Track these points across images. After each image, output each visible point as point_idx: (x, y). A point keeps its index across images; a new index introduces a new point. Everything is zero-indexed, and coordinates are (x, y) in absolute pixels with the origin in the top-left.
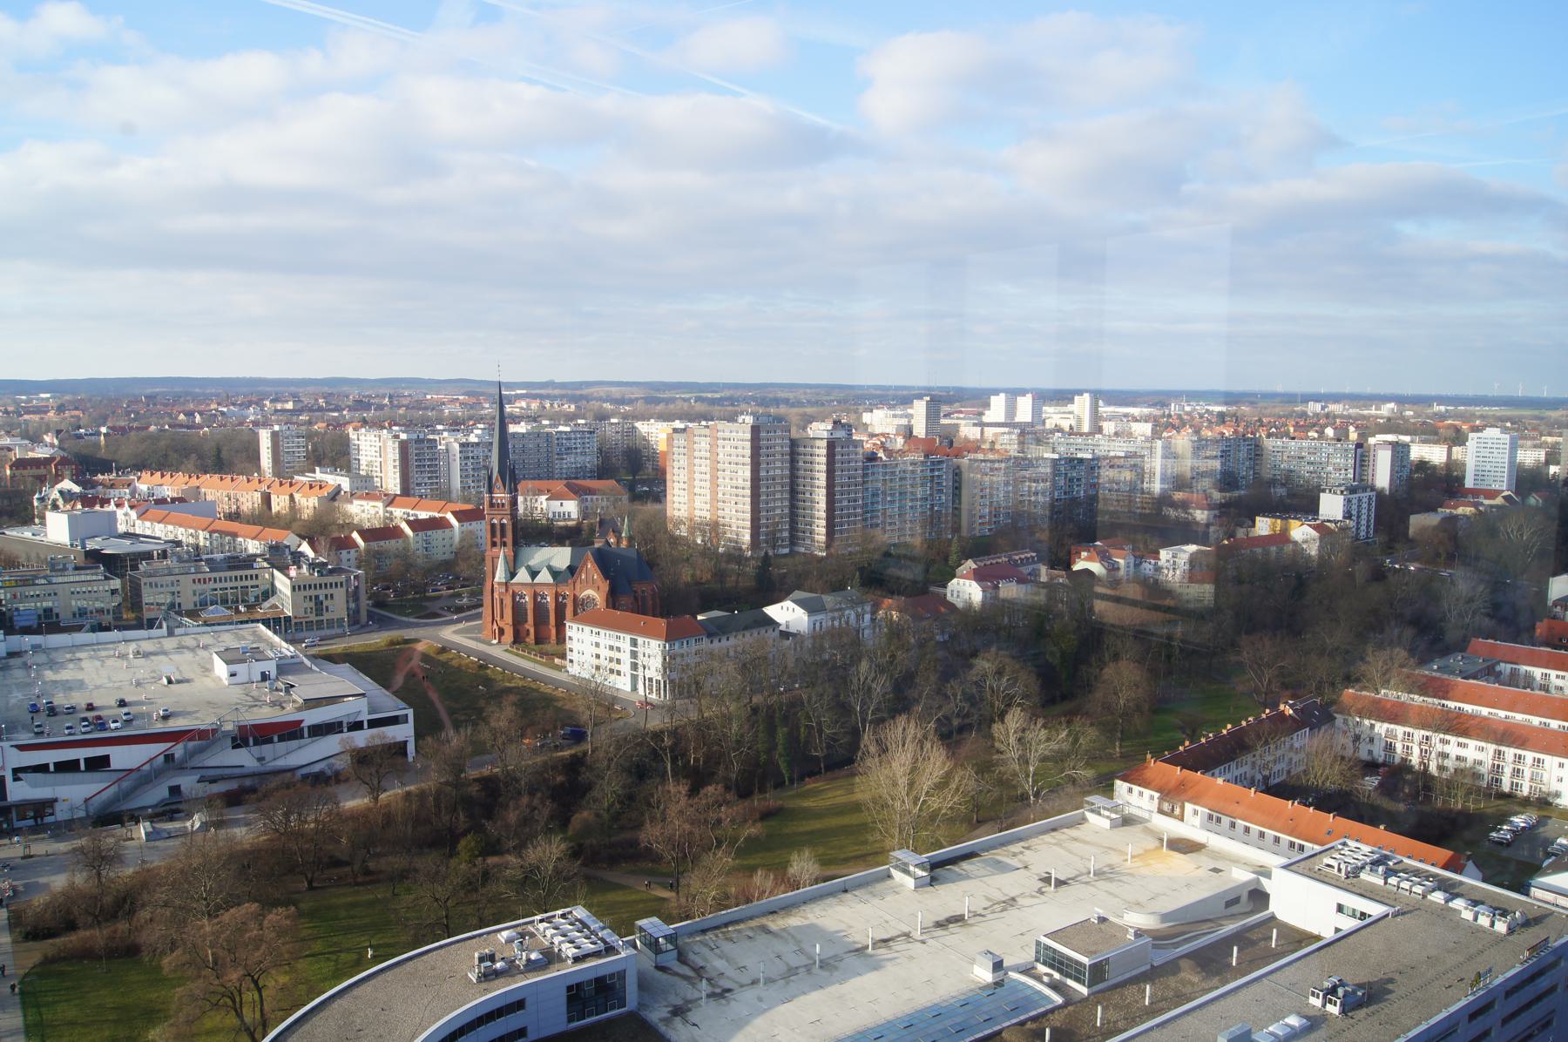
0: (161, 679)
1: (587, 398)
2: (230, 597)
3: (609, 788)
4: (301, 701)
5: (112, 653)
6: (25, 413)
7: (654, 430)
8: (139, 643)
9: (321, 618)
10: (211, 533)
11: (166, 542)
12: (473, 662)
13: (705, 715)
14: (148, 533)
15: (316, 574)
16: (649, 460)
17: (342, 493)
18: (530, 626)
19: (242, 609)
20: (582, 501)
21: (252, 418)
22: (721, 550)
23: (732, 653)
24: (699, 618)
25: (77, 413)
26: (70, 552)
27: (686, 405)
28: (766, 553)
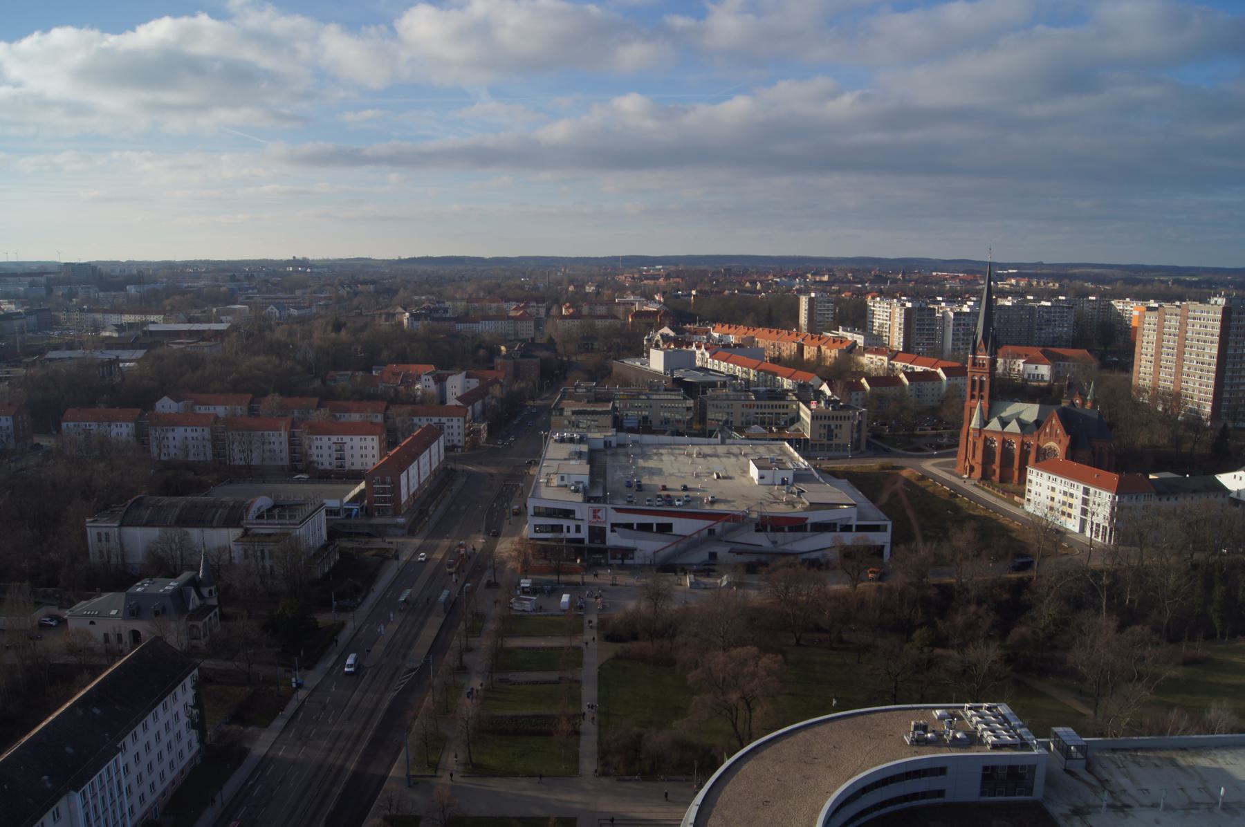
0: (712, 474)
1: (1072, 277)
2: (767, 420)
3: (1047, 611)
4: (808, 504)
5: (682, 452)
6: (645, 279)
7: (1128, 308)
8: (701, 447)
9: (830, 442)
10: (759, 371)
11: (727, 376)
13: (1146, 563)
14: (716, 368)
15: (830, 408)
16: (1121, 334)
17: (857, 347)
18: (996, 467)
19: (774, 429)
21: (797, 287)
22: (1179, 418)
23: (1178, 512)
24: (1151, 477)
25: (678, 280)
26: (663, 378)
27: (1163, 287)
28: (1225, 426)
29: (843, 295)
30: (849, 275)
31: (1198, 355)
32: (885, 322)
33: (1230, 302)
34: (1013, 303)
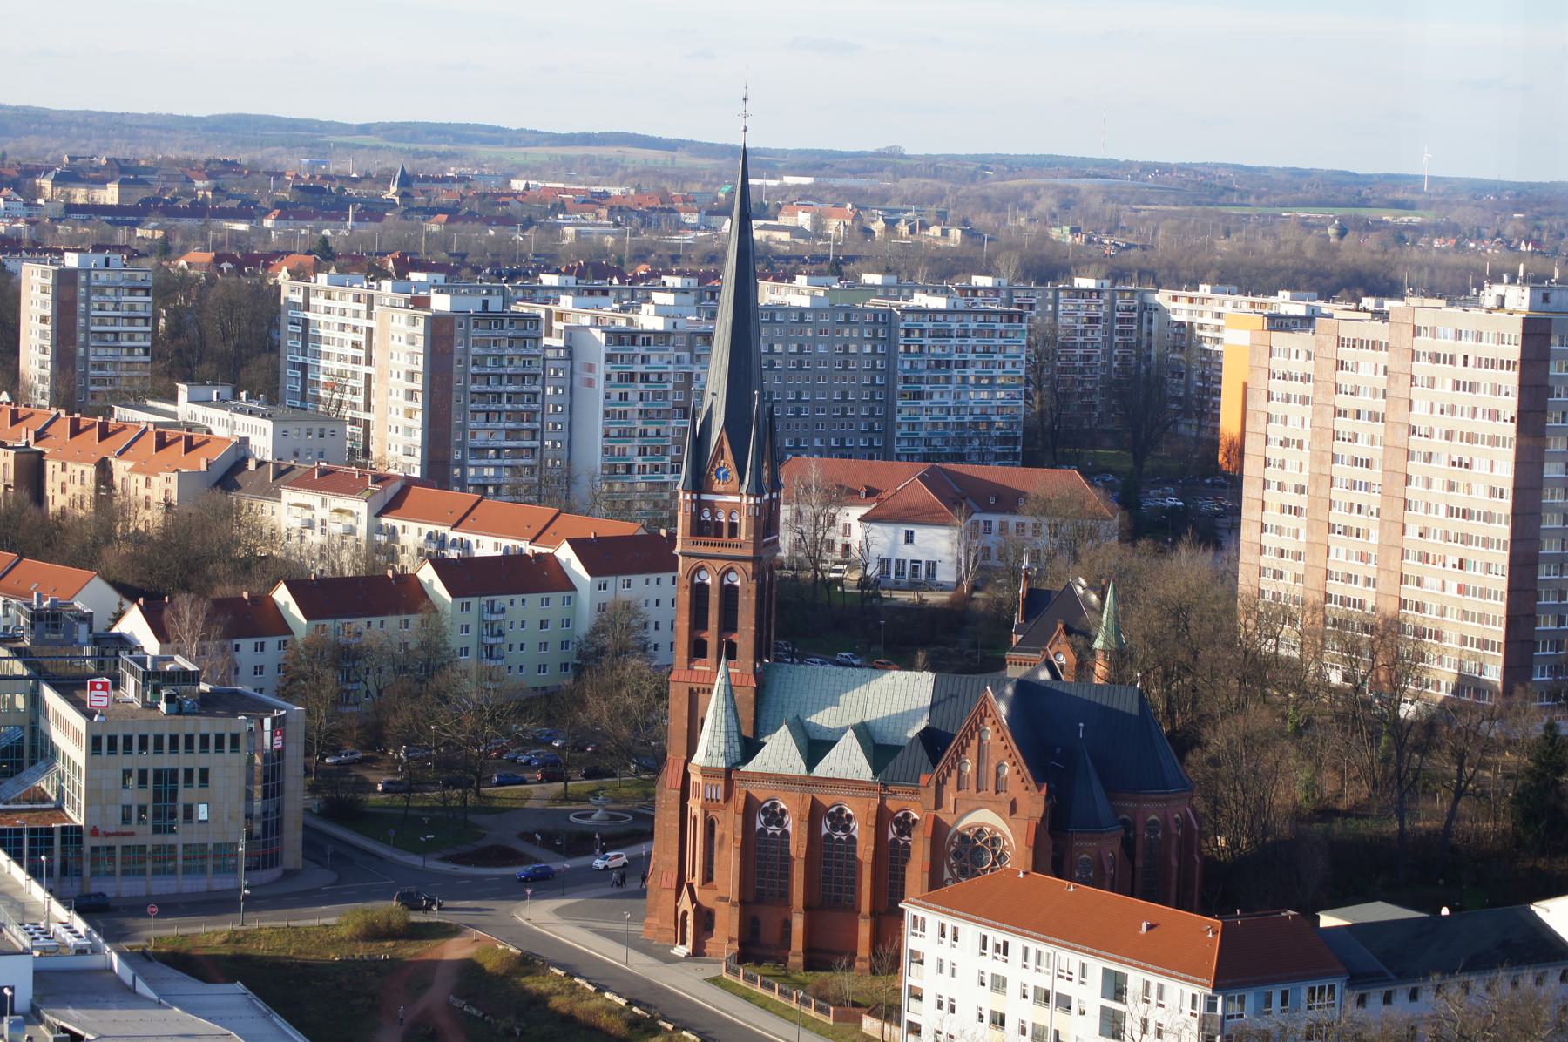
7: (1207, 319)
9: (160, 839)
12: (613, 1010)
15: (163, 706)
16: (1187, 413)
17: (252, 465)
20: (974, 532)
22: (1407, 711)
24: (1327, 920)
29: (182, 263)
30: (199, 184)
31: (1451, 487)
32: (350, 367)
33: (1546, 298)
34: (813, 296)
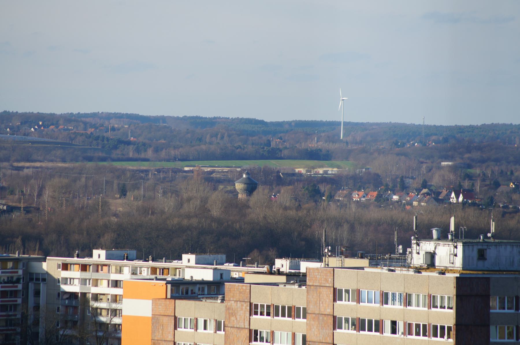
7: (103, 288)
33: (482, 255)
